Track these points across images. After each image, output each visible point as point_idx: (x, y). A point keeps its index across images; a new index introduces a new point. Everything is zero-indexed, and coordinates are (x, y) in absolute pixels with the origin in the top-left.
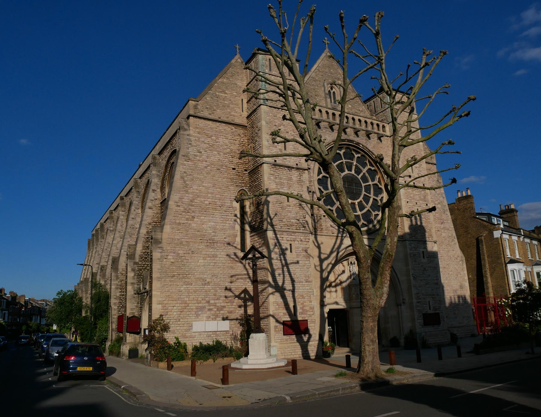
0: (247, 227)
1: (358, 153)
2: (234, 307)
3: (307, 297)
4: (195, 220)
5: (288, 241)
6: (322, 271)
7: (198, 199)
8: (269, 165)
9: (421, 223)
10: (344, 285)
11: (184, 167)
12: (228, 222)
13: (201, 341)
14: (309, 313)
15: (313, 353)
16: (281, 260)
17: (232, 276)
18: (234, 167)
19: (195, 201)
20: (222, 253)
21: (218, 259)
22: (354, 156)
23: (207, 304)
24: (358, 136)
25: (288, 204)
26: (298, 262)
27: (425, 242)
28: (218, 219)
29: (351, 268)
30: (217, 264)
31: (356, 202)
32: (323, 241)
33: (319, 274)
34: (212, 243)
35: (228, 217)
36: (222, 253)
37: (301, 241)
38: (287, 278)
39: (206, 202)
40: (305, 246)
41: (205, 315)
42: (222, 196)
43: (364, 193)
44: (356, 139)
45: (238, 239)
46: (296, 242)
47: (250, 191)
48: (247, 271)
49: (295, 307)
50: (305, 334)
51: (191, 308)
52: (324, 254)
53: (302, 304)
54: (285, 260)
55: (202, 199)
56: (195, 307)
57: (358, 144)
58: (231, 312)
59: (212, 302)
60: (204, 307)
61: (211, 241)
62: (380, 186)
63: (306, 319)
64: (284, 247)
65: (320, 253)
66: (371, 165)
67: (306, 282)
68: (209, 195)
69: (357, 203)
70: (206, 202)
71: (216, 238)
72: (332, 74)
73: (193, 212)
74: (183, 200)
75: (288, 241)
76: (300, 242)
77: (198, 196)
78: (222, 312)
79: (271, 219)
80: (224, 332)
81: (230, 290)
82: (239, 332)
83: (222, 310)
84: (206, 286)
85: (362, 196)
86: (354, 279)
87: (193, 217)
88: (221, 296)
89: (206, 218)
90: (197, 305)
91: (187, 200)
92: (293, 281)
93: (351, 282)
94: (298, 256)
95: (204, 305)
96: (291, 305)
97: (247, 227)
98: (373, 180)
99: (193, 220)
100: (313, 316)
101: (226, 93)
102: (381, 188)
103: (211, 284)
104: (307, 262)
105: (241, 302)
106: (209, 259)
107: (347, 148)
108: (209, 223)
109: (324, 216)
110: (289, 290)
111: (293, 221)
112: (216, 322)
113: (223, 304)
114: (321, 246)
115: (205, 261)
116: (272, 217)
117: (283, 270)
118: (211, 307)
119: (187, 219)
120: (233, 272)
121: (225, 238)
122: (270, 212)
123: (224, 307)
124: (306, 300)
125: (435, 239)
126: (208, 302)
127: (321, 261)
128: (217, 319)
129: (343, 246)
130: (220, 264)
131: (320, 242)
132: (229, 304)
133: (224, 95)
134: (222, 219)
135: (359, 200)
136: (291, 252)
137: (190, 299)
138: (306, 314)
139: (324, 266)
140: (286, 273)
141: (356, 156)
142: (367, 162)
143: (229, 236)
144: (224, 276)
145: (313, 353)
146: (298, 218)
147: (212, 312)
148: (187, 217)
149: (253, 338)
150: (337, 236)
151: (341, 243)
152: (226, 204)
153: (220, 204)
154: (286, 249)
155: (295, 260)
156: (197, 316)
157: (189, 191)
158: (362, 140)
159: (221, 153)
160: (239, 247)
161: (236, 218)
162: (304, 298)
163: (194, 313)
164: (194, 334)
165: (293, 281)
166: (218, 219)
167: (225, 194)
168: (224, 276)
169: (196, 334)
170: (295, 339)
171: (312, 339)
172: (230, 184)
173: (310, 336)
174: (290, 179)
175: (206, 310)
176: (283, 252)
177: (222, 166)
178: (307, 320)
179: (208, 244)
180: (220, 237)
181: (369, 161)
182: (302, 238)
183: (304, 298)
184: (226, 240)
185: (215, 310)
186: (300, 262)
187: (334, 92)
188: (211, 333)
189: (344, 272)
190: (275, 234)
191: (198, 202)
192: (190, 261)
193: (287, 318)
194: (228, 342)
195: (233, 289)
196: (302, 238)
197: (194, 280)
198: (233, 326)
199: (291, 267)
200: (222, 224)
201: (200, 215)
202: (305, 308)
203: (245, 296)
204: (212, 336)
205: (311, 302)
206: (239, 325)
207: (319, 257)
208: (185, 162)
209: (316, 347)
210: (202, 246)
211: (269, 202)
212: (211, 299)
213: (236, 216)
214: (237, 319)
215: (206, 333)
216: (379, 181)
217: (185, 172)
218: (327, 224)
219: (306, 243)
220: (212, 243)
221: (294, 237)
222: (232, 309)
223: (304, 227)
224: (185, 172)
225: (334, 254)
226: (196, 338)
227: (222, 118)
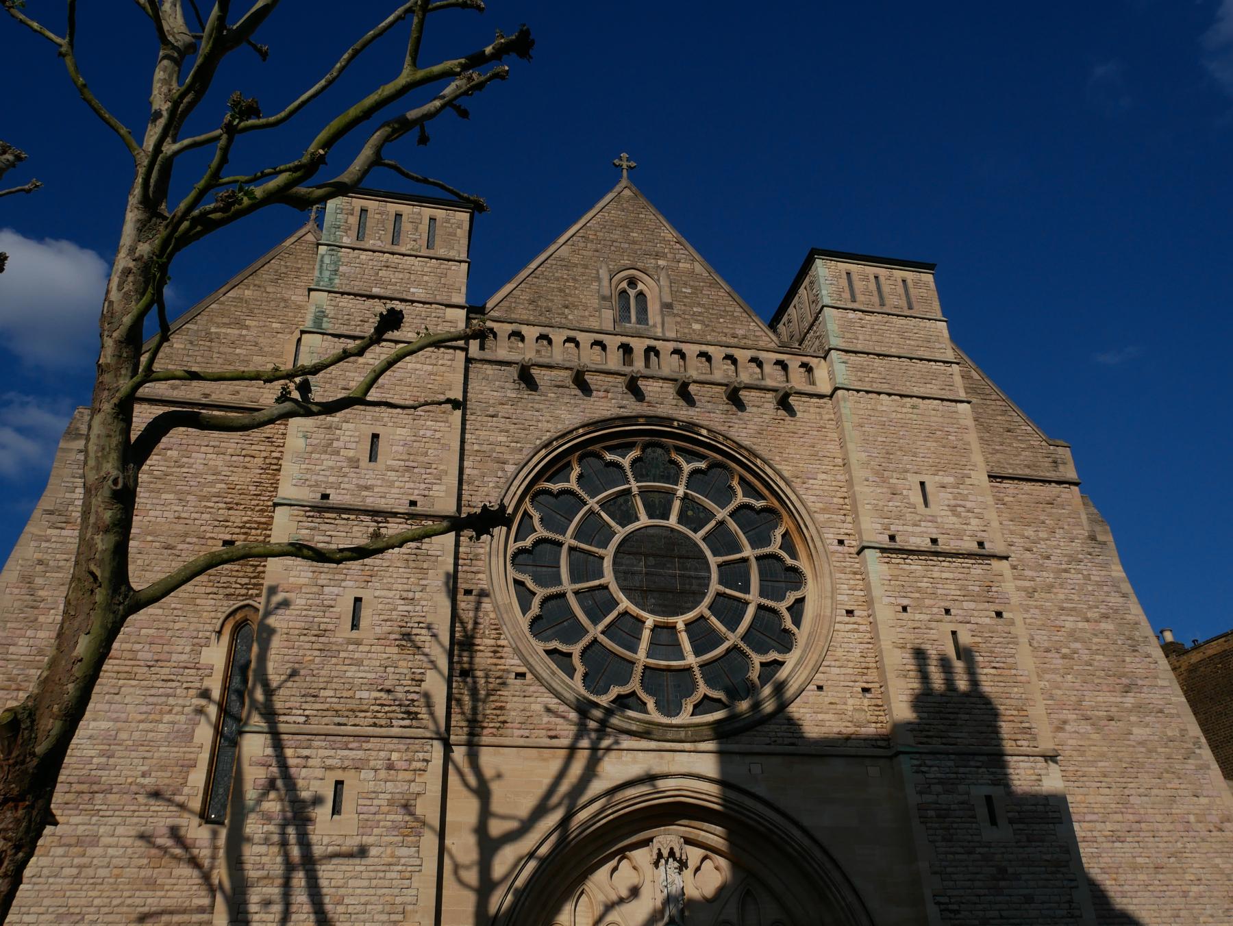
8: (295, 511)
9: (974, 682)
11: (44, 545)
12: (167, 718)
16: (284, 844)
18: (228, 537)
20: (120, 830)
21: (98, 851)
24: (689, 400)
26: (362, 852)
27: (996, 759)
32: (504, 769)
35: (171, 701)
44: (684, 413)
46: (366, 774)
54: (305, 843)
57: (691, 426)
61: (84, 787)
64: (305, 795)
65: (485, 813)
71: (107, 777)
72: (634, 242)
74: (12, 649)
75: (329, 768)
76: (383, 774)
79: (269, 692)
91: (25, 650)
94: (365, 826)
101: (247, 328)
104: (403, 851)
106: (60, 851)
109: (520, 675)
111: (365, 695)
114: (495, 787)
116: (274, 684)
117: (287, 884)
120: (153, 901)
121: (143, 775)
122: (270, 666)
125: (1046, 745)
127: (488, 846)
130: (102, 872)
131: (488, 772)
133: (237, 332)
134: (144, 708)
136: (336, 810)
139: (500, 868)
140: (301, 898)
141: (687, 468)
142: (735, 483)
143: (163, 768)
146: (388, 684)
150: (572, 749)
151: (590, 772)
153: (149, 656)
154: (318, 801)
155: (352, 843)
157: (41, 619)
158: (709, 414)
159: (189, 498)
161: (203, 702)
176: (299, 813)
177: (186, 535)
181: (742, 480)
182: (395, 756)
184: (146, 781)
186: (373, 851)
187: (641, 294)
190: (278, 745)
199: (328, 874)
208: (49, 531)
211: (272, 631)
213: (205, 694)
217: (40, 562)
219: (409, 775)
221: (360, 754)
223: (413, 716)
224: (40, 562)
227: (214, 397)
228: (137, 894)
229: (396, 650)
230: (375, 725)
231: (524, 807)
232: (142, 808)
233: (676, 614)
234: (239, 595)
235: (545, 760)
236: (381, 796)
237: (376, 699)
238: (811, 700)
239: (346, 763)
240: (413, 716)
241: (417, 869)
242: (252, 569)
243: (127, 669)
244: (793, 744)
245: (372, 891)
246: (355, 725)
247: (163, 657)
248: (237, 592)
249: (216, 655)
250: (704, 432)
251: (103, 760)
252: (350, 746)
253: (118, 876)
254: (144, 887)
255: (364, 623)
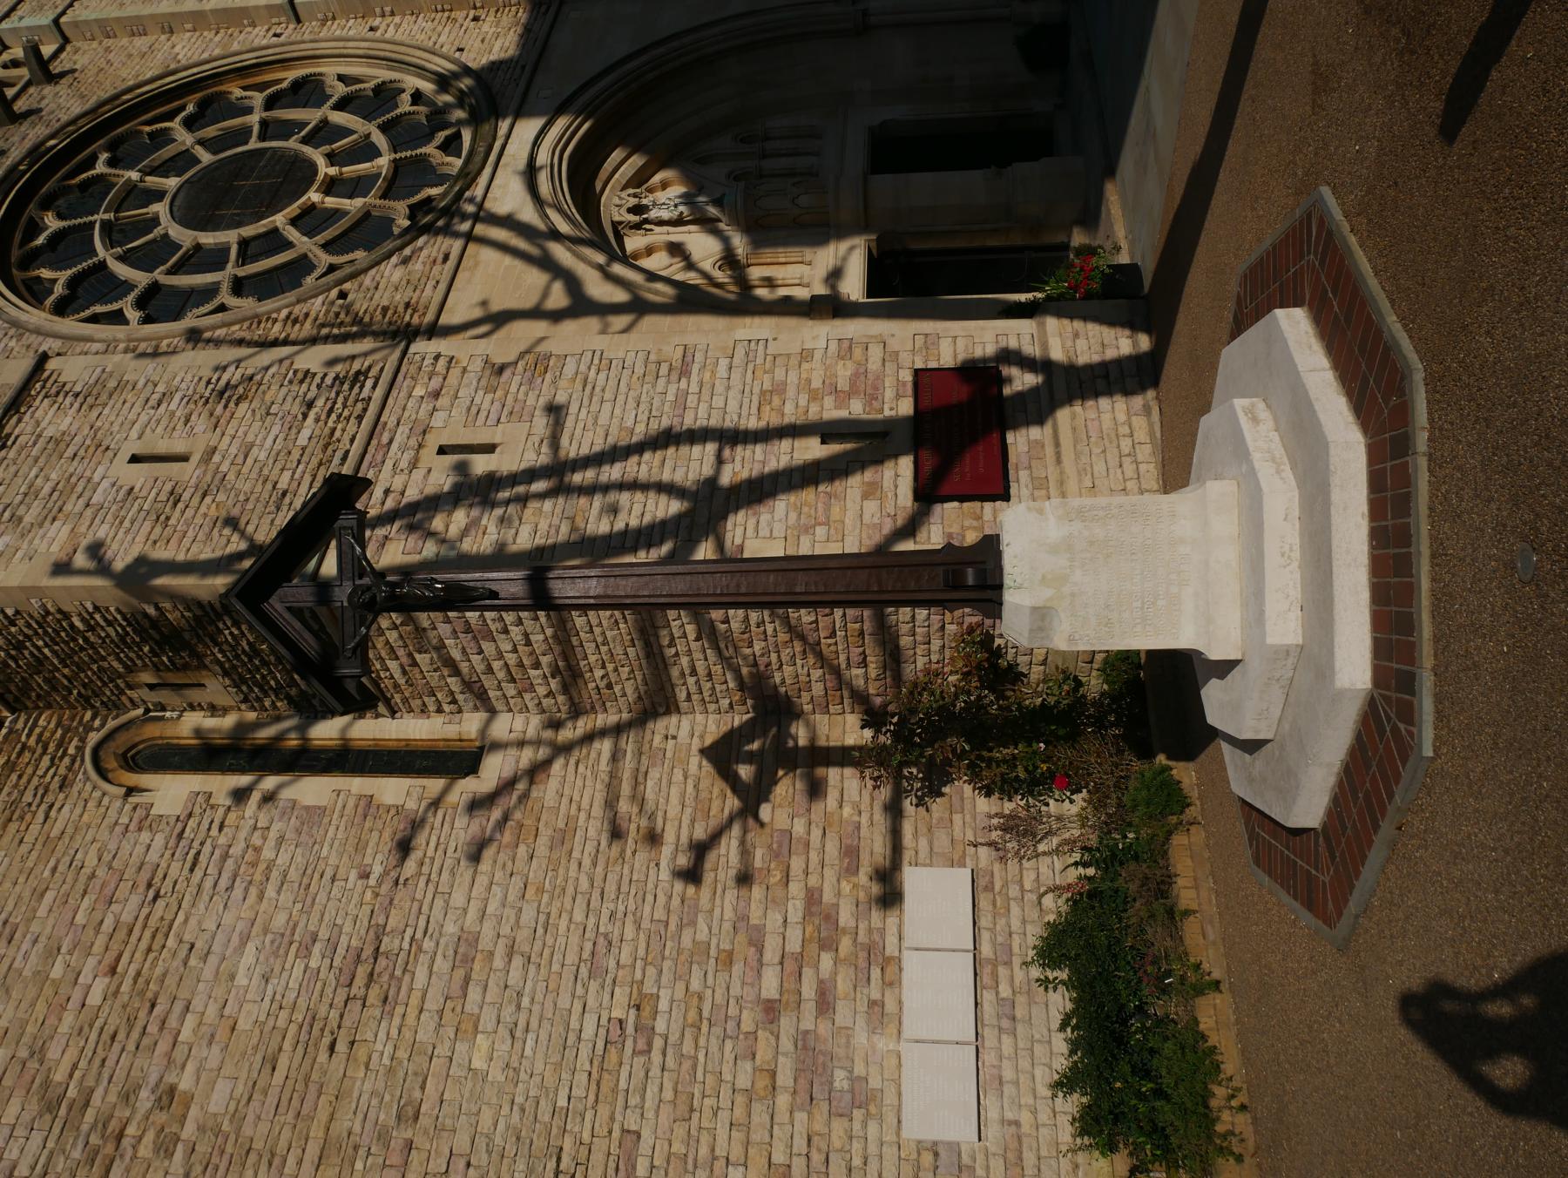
0: (326, 731)
1: (91, 162)
2: (816, 833)
3: (779, 374)
4: (185, 1083)
5: (414, 465)
6: (639, 307)
7: (53, 1052)
10: (739, 243)
12: (268, 854)
13: (1044, 1077)
14: (874, 365)
15: (1122, 343)
17: (616, 834)
19: (59, 1076)
20: (458, 899)
21: (487, 930)
22: (101, 177)
23: (786, 1023)
25: (195, 459)
26: (555, 411)
28: (228, 919)
29: (665, 215)
30: (523, 935)
31: (325, 169)
32: (477, 298)
33: (649, 321)
34: (371, 970)
36: (464, 900)
37: (436, 395)
38: (645, 467)
39: (95, 998)
40: (471, 377)
41: (861, 1038)
42: (97, 883)
43: (292, 143)
45: (393, 790)
47: (115, 707)
48: (602, 733)
49: (827, 431)
50: (1002, 381)
51: (800, 1144)
52: (546, 294)
53: (815, 396)
54: (531, 475)
55: (68, 1019)
56: (801, 1116)
57: (35, 152)
58: (851, 854)
59: (770, 985)
60: (804, 1041)
61: (362, 972)
62: (284, 85)
63: (907, 377)
65: (536, 313)
66: (170, 116)
67: (685, 372)
68: (57, 972)
69: (333, 171)
70: (95, 998)
71: (352, 936)
73: (127, 1097)
75: (414, 465)
76: (443, 401)
77: (39, 1053)
78: (845, 917)
80: (984, 903)
81: (701, 850)
82: (984, 805)
83: (831, 918)
84: (660, 1026)
85: (308, 150)
86: (718, 202)
87: (168, 1096)
88: (742, 918)
89: (197, 1004)
90: (783, 1100)
91: (37, 1138)
92: (666, 439)
93: (736, 222)
95: (786, 1044)
96: (812, 449)
97: (326, 731)
98: (249, 111)
99: (188, 1100)
100: (893, 345)
102: (297, 85)
103: (649, 988)
105: (787, 788)
106: (474, 993)
107: (46, 205)
108: (241, 980)
109: (343, 295)
110: (720, 461)
111: (306, 433)
112: (911, 961)
113: (795, 909)
114: (496, 307)
115: (488, 1021)
116: (243, 546)
117: (590, 490)
118: (808, 990)
119: (165, 1147)
120: (593, 828)
121: (365, 876)
122: (207, 554)
123: (812, 898)
124: (793, 378)
126: (771, 1010)
127: (581, 306)
128: (891, 950)
129: (529, 214)
130: (528, 914)
131: (477, 313)
132: (797, 864)
134: (238, 892)
135: (321, 162)
136: (490, 449)
137: (736, 1153)
138: (880, 378)
139: (620, 296)
140: (613, 472)
142: (147, 129)
143: (360, 847)
144: (611, 888)
145: (1122, 343)
146: (297, 409)
147: (843, 985)
148: (145, 1151)
149: (1041, 615)
151: (508, 222)
152: (153, 856)
153: (135, 900)
154: (461, 468)
155: (541, 424)
156: (862, 1099)
160: (435, 785)
161: (256, 797)
162: (780, 389)
163: (838, 1126)
164: (993, 1132)
165: (666, 439)
166: (228, 919)
167: (91, 860)
168: (611, 888)
169: (992, 1113)
170: (1035, 432)
171: (1031, 349)
172: (35, 828)
173: (1009, 356)
174: (58, 443)
175: (824, 1028)
176: (478, 491)
178: (917, 372)
179: (374, 995)
180: (346, 912)
182: (419, 391)
183: (780, 389)
184: (377, 870)
185: (826, 960)
186: (561, 398)
188: (988, 997)
189: (676, 249)
191: (71, 1054)
192: (462, 1142)
193: (899, 475)
194: (1047, 879)
195: (700, 833)
196: (419, 391)
197: (604, 1111)
198: (942, 841)
200: (271, 892)
201: (163, 1047)
202: (843, 384)
203: (750, 758)
204: (1005, 991)
205: (806, 355)
206: (938, 806)
207: (556, 316)
209: (1078, 324)
210: (380, 1040)
211: (141, 561)
212: (749, 993)
213: (240, 795)
214: (894, 810)
215: (989, 1034)
216: (260, 87)
218: (387, 284)
219: (455, 373)
220: (371, 970)
221: (403, 431)
222: (832, 848)
223: (359, 377)
225: (560, 252)
226: (1025, 1118)
228: (576, 854)
229: (244, 406)
230: (360, 418)
231: (536, 278)
232: (425, 870)
233: (316, 172)
234: (69, 769)
235: (477, 264)
236: (477, 400)
237: (317, 420)
238: (472, 55)
239: (413, 442)
240: (359, 377)
241: (598, 354)
242: (27, 754)
243: (148, 934)
244: (523, 67)
245: (621, 398)
246: (352, 441)
247: (144, 876)
248: (62, 771)
249: (171, 792)
250: (52, 142)
251: (317, 949)
252: (385, 440)
253: (541, 890)
254: (567, 847)
255: (179, 447)
